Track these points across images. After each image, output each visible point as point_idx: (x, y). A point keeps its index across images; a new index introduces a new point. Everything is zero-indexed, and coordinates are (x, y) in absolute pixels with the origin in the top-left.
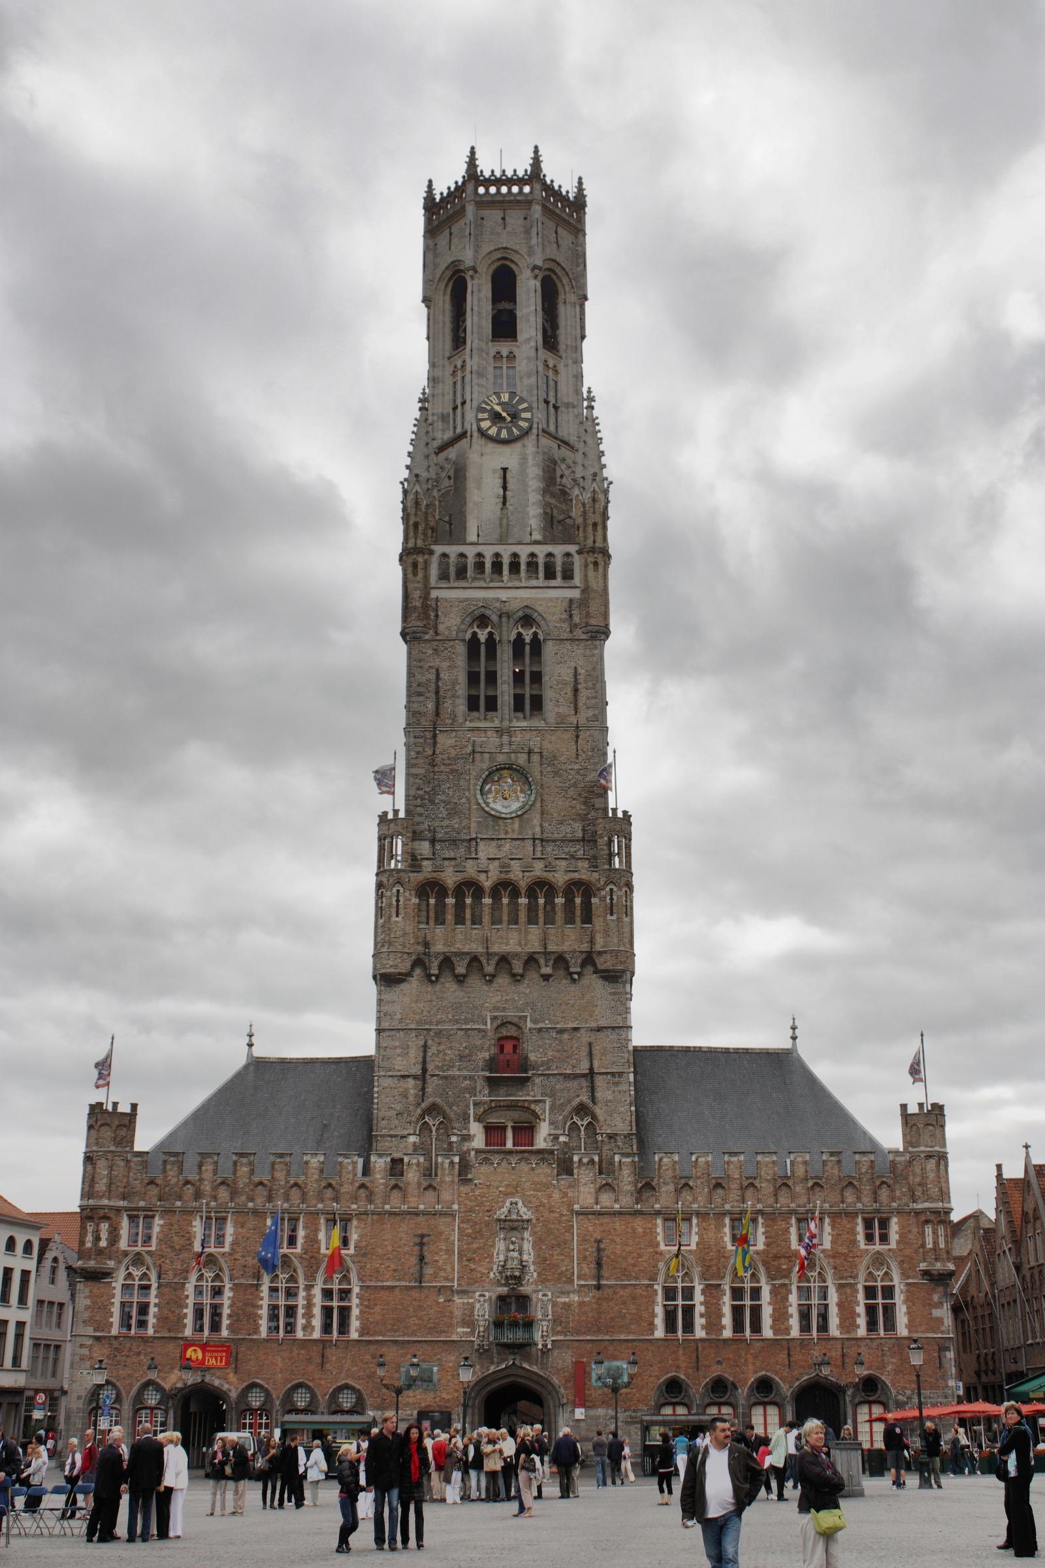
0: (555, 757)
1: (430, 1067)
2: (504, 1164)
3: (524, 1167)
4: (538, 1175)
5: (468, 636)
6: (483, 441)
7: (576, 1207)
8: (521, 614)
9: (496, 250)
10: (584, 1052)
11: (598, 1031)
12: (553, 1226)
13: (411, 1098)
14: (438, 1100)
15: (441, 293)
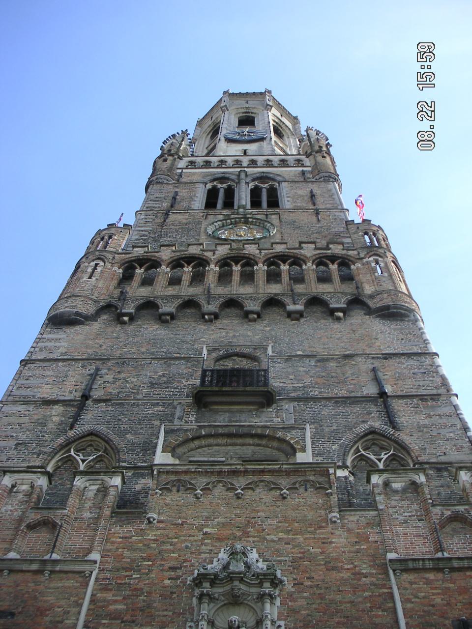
0: (295, 222)
1: (96, 394)
2: (219, 490)
3: (262, 495)
4: (296, 508)
5: (209, 186)
6: (229, 144)
7: (391, 556)
8: (258, 175)
9: (241, 108)
10: (365, 378)
11: (386, 358)
12: (339, 598)
13: (51, 426)
14: (102, 428)
15: (204, 138)
